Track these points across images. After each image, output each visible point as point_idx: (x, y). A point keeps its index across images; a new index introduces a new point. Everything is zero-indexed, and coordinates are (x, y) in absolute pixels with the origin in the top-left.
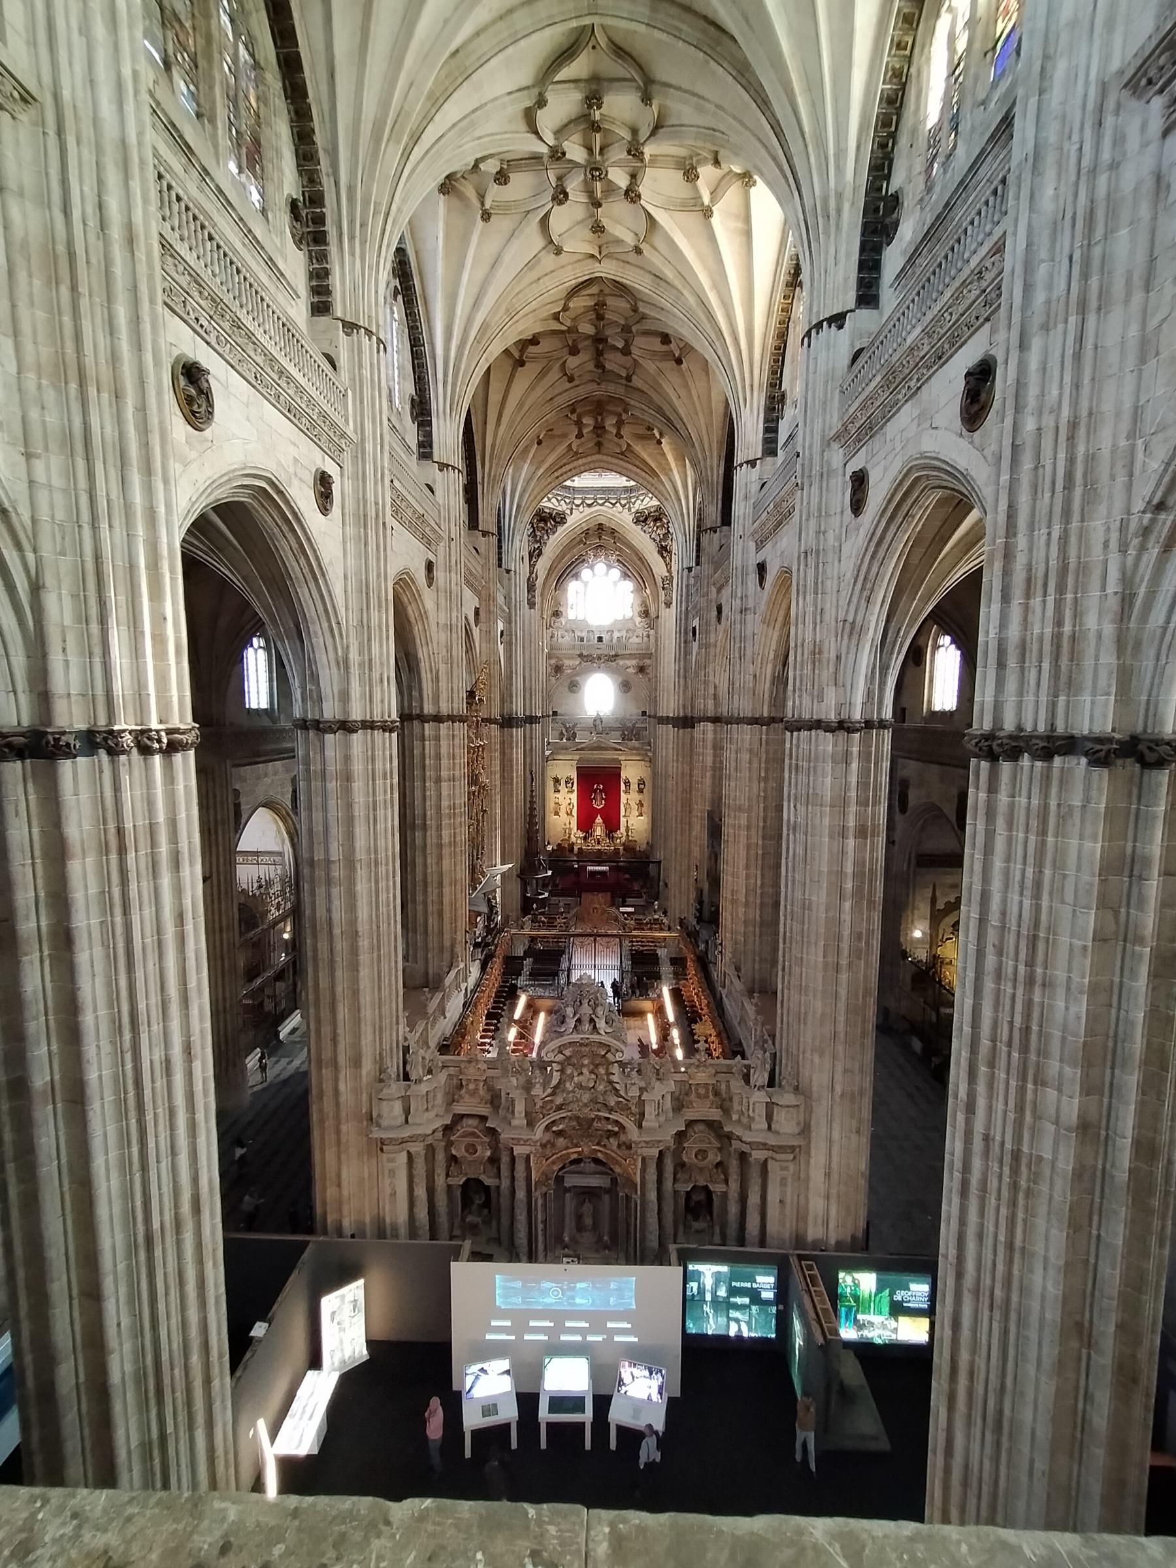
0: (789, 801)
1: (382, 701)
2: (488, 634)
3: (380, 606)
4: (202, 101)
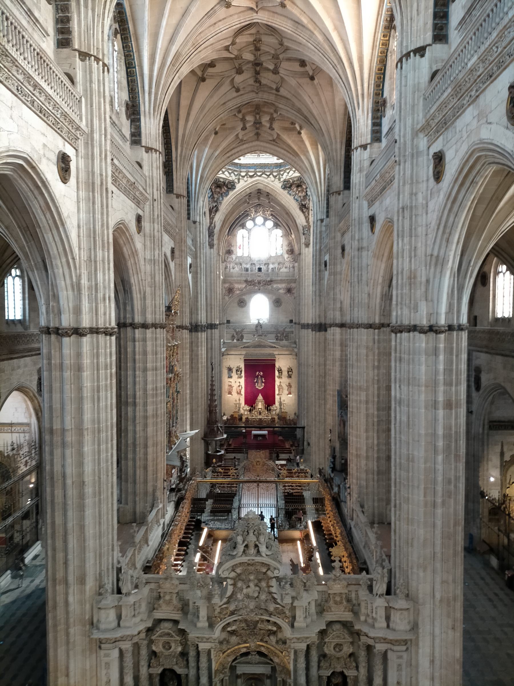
0: (395, 382)
1: (105, 314)
2: (181, 266)
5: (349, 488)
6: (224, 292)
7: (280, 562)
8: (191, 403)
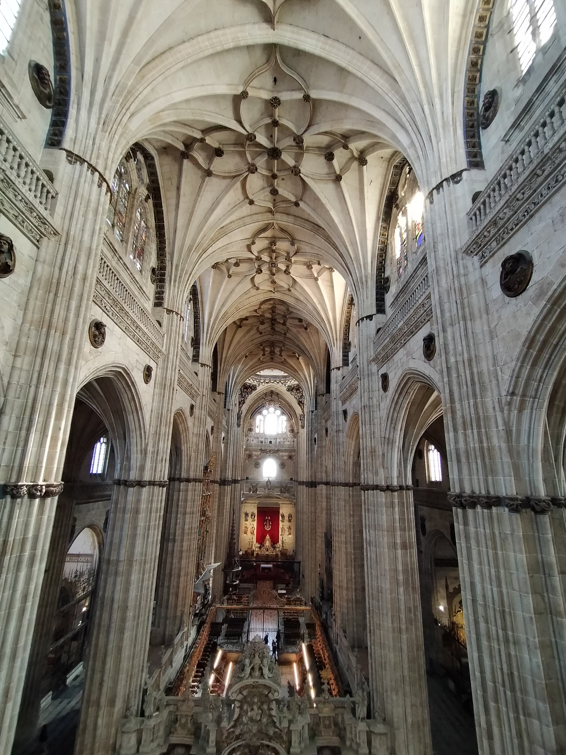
0: (366, 528)
1: (161, 471)
2: (217, 439)
3: (166, 425)
4: (124, 237)
5: (334, 615)
6: (245, 457)
7: (279, 684)
8: (216, 541)
